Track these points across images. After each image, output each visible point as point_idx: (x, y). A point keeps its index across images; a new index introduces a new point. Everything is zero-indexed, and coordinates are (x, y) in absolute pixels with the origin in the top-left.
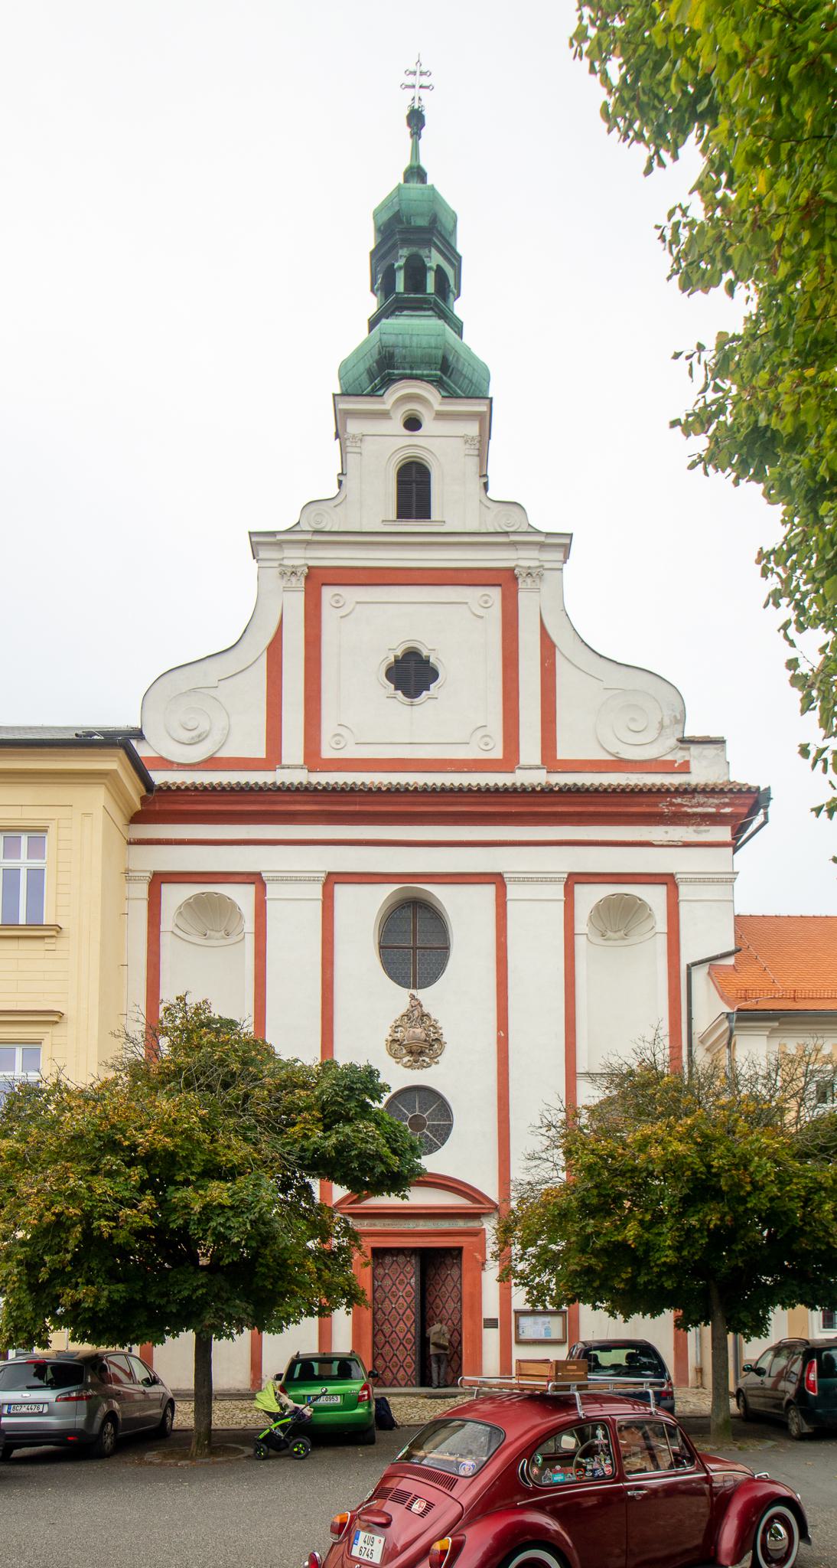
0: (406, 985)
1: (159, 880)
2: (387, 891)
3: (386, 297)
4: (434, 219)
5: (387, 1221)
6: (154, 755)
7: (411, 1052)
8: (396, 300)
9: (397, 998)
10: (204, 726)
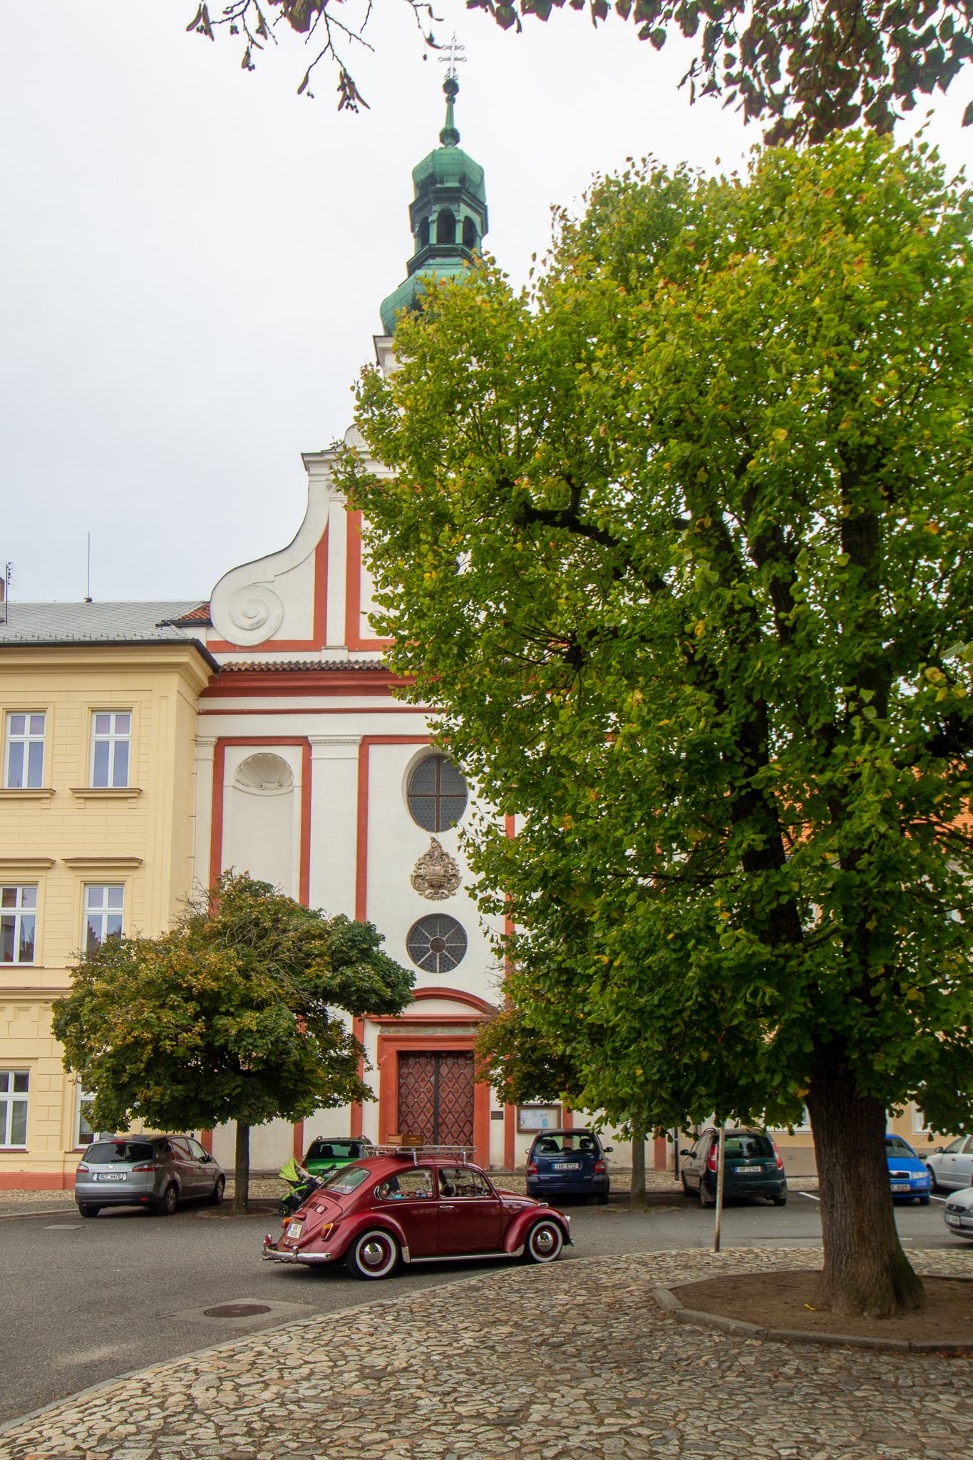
0: (429, 829)
1: (223, 743)
2: (413, 750)
3: (423, 246)
4: (463, 179)
5: (410, 1029)
6: (218, 639)
7: (432, 886)
8: (430, 250)
9: (422, 839)
10: (262, 614)
